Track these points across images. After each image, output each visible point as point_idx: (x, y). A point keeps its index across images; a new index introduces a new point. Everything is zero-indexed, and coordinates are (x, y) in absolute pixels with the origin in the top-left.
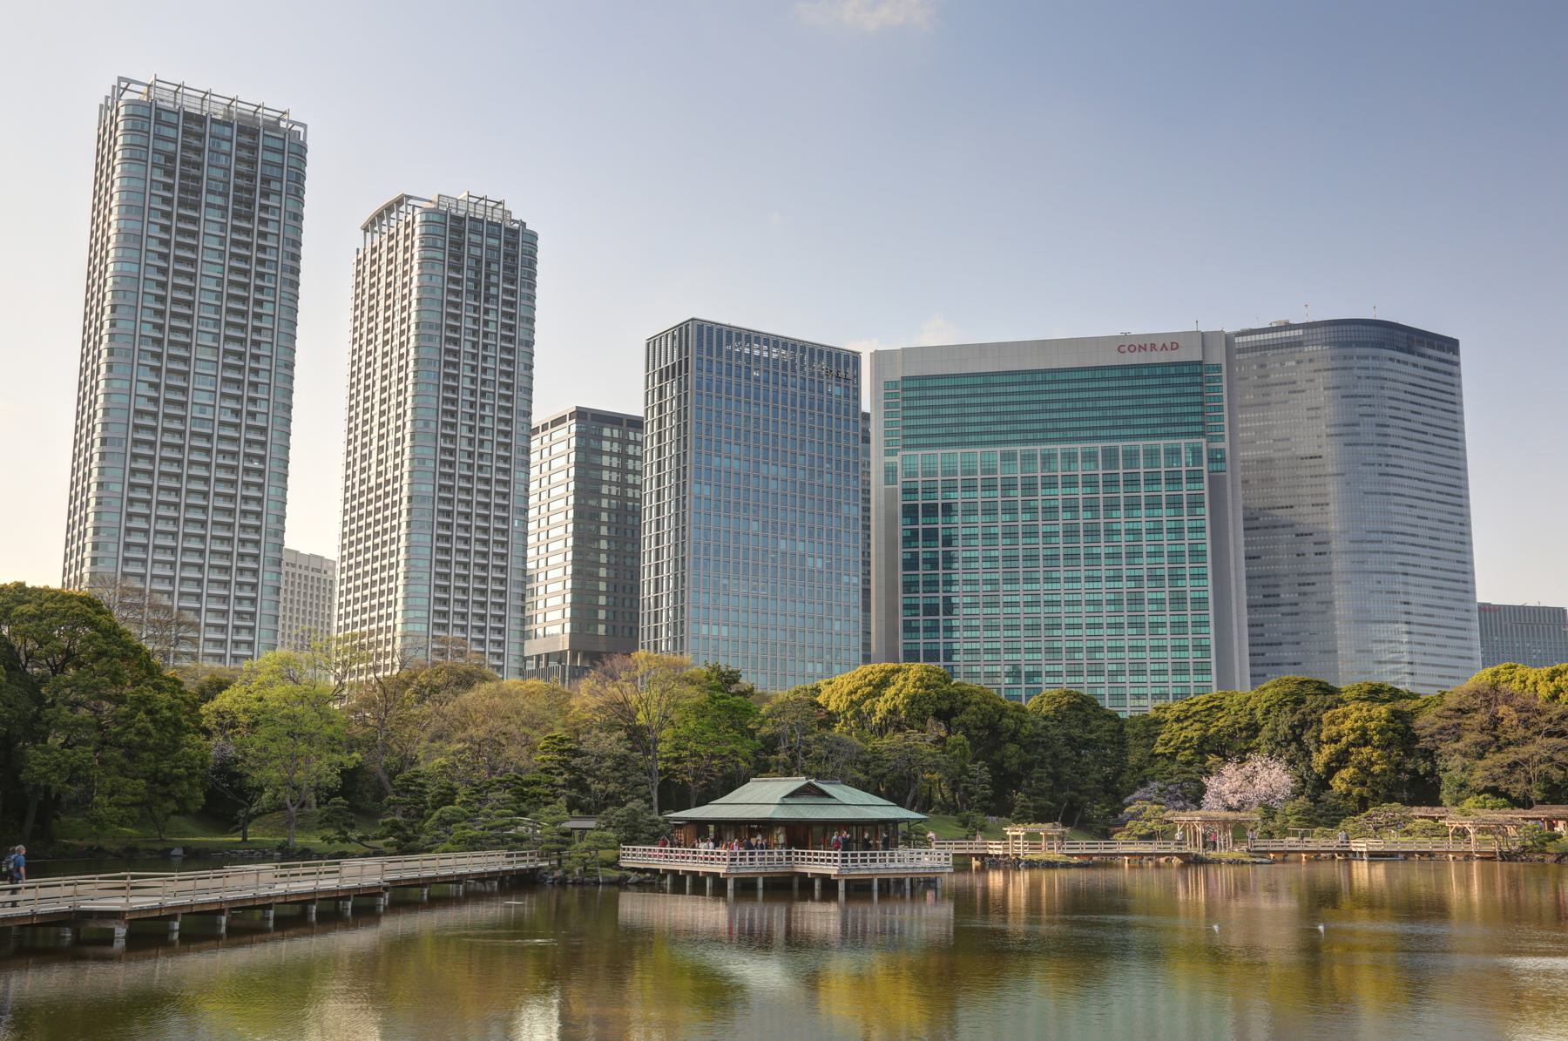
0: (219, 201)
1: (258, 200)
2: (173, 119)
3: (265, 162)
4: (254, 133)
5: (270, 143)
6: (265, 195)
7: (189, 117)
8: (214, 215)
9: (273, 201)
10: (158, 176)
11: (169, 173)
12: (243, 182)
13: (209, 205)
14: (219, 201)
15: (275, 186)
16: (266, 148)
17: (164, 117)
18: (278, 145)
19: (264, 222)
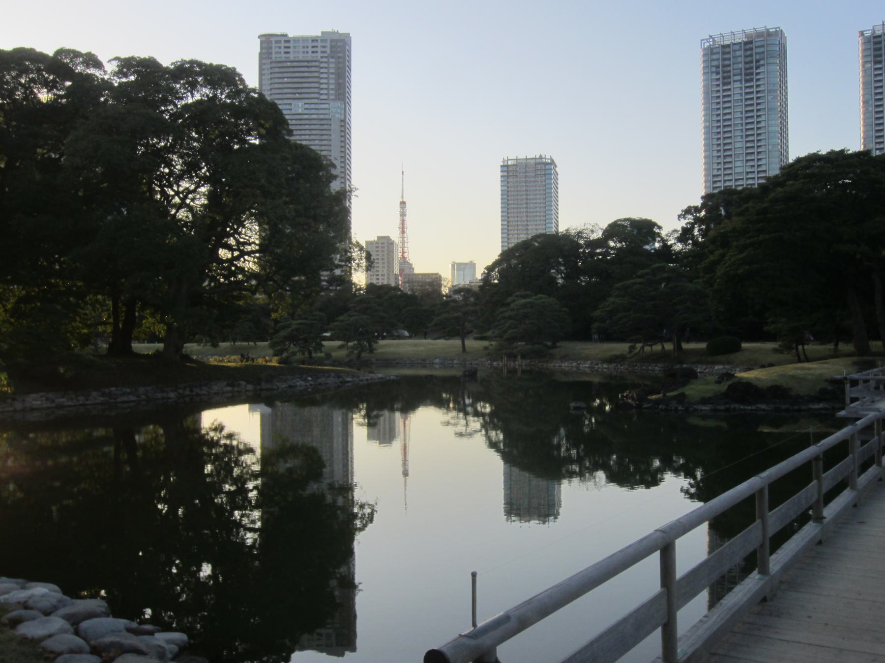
0: (738, 78)
1: (754, 71)
2: (718, 50)
3: (756, 54)
4: (751, 42)
5: (758, 44)
6: (757, 68)
7: (724, 47)
8: (738, 85)
9: (761, 70)
10: (714, 76)
11: (718, 73)
12: (748, 66)
13: (734, 81)
14: (738, 78)
15: (762, 62)
16: (756, 47)
17: (715, 51)
18: (762, 43)
19: (758, 80)
